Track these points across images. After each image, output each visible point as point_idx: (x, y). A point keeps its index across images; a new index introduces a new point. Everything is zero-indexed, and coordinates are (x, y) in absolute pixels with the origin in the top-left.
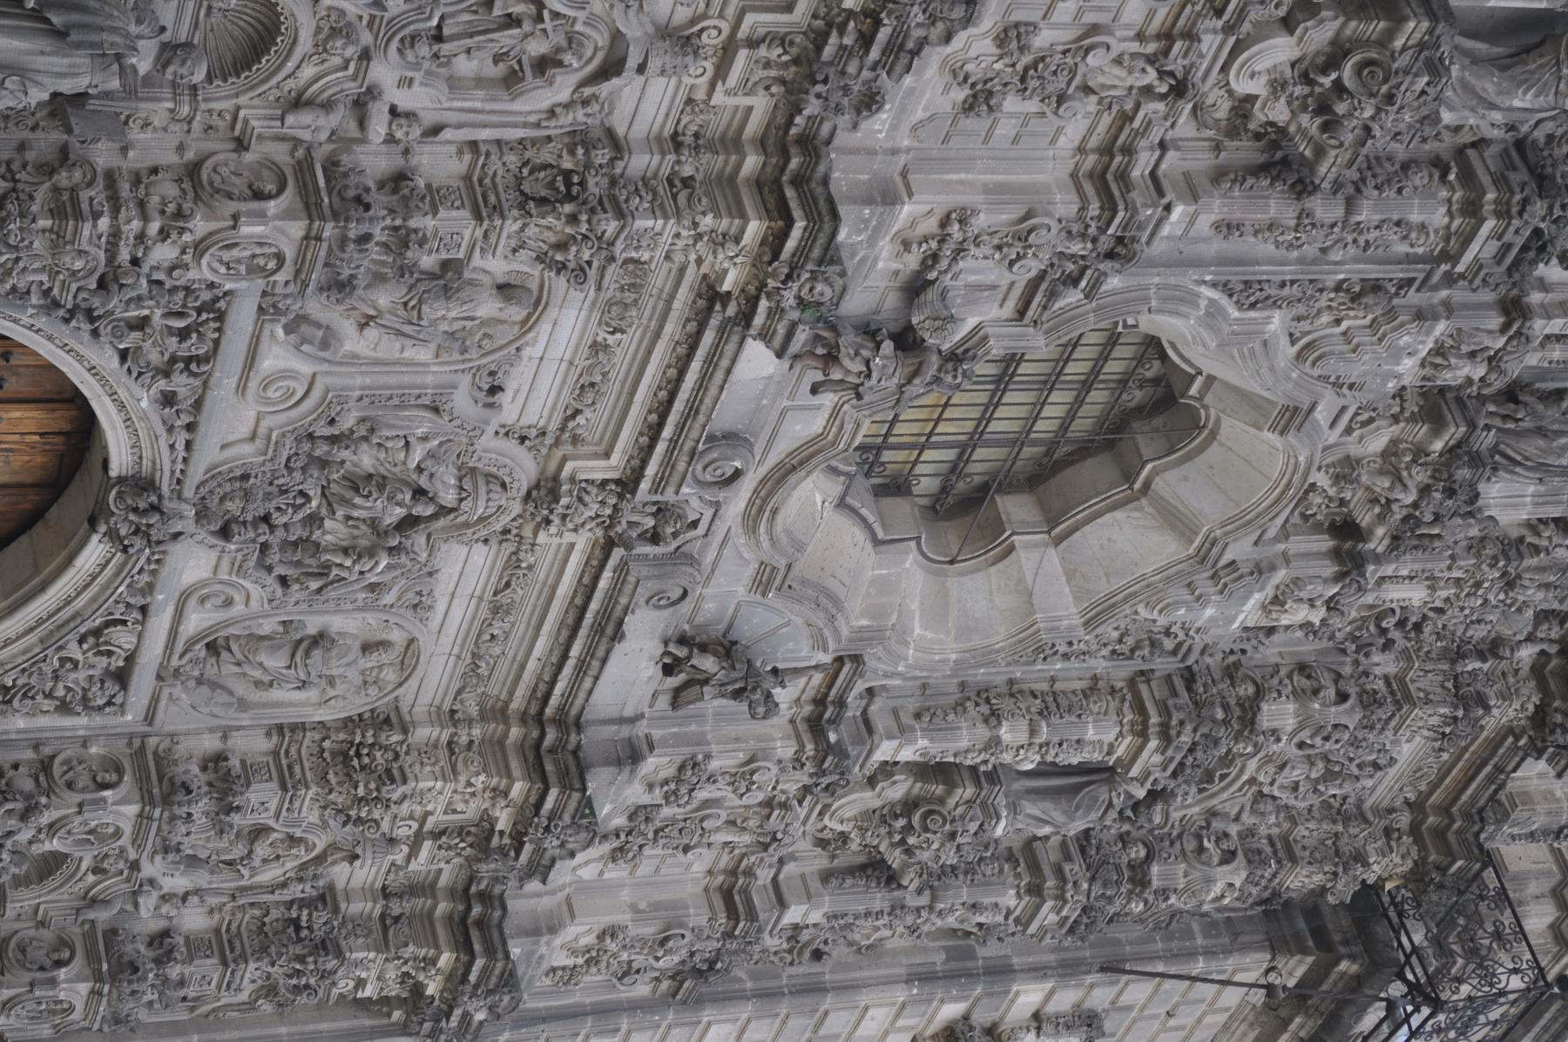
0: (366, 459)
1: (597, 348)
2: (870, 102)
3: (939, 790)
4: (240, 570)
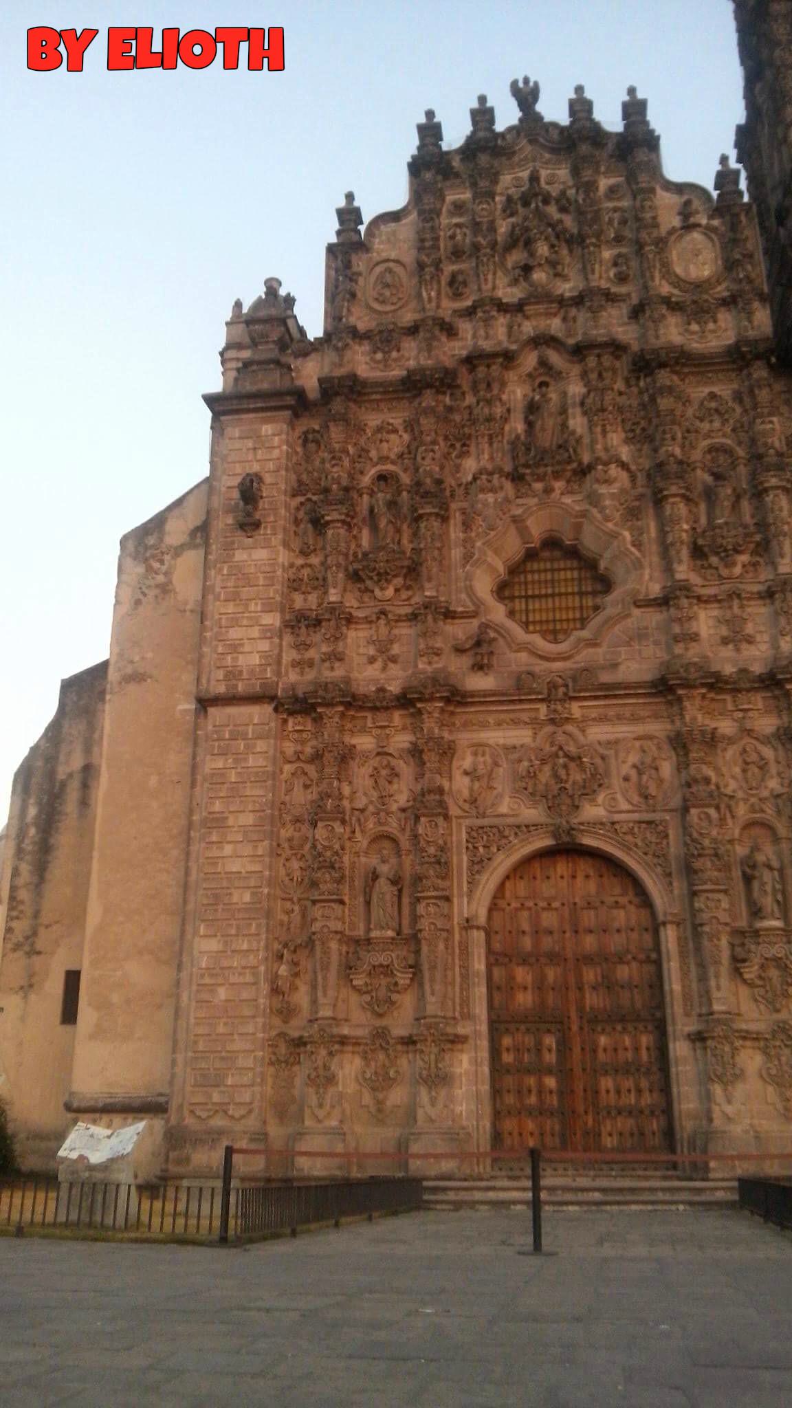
0: (545, 775)
1: (499, 724)
2: (382, 690)
3: (706, 549)
4: (594, 800)
